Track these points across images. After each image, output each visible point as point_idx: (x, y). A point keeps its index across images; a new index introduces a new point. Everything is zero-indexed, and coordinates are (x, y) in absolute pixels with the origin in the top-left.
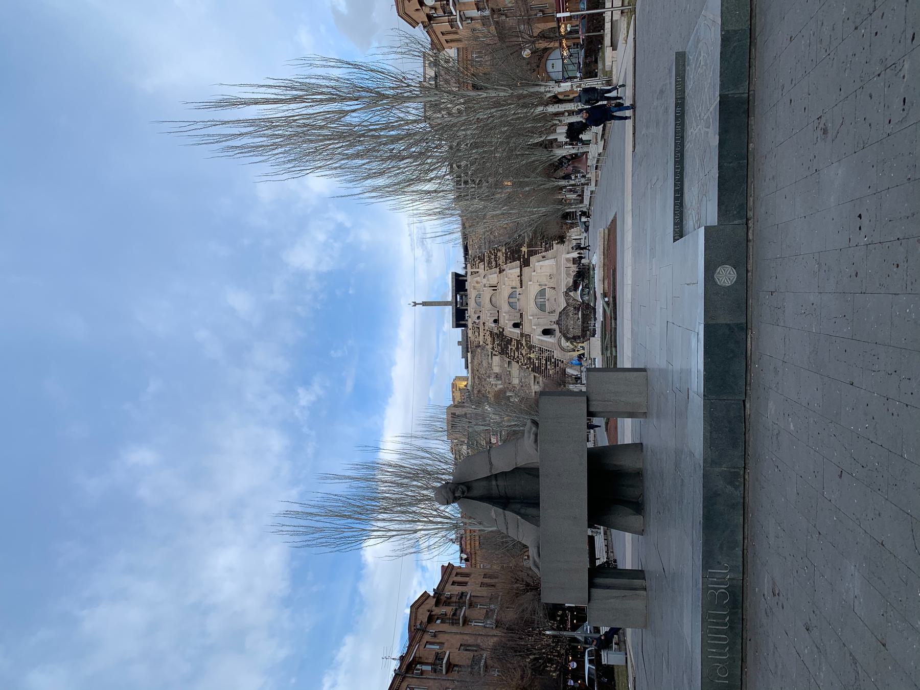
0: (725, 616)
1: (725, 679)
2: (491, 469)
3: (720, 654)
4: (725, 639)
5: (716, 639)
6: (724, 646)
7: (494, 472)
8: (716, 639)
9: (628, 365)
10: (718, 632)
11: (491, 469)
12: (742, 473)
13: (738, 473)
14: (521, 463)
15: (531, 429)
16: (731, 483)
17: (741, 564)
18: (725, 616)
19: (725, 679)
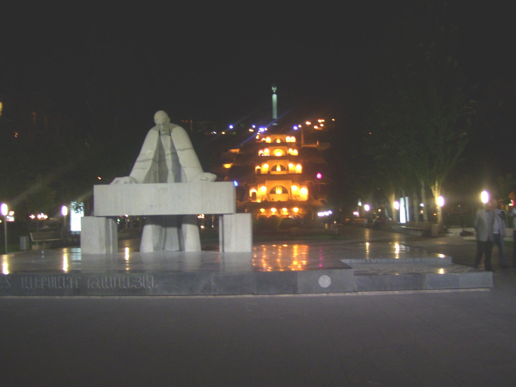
3: (104, 284)
4: (113, 286)
5: (113, 281)
6: (109, 285)
7: (179, 153)
8: (113, 281)
10: (117, 282)
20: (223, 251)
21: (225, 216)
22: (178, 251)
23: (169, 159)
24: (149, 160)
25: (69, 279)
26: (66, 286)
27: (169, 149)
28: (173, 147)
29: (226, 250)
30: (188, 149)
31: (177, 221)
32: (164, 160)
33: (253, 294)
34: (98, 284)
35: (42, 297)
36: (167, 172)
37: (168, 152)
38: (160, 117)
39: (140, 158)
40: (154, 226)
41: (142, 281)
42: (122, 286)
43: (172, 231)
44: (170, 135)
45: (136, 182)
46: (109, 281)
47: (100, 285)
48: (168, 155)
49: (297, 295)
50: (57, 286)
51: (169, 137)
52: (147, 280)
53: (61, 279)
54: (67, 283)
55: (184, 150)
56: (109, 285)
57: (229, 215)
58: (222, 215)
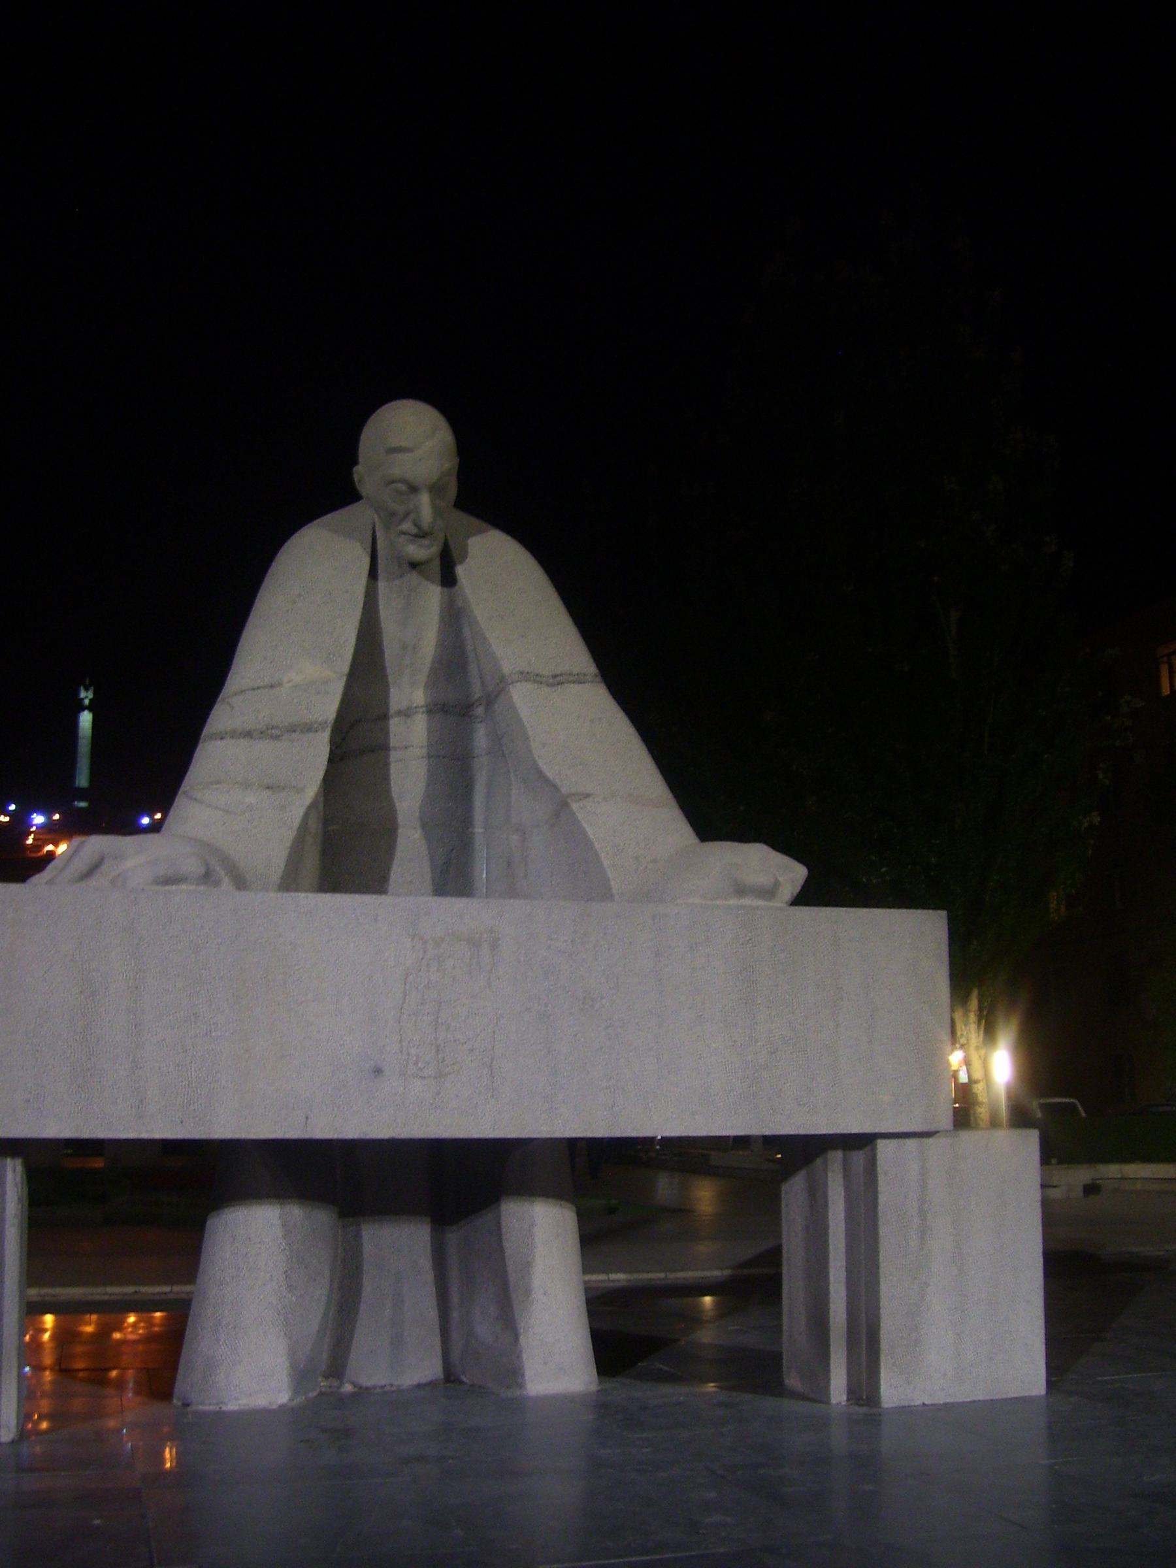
20: (865, 1390)
21: (884, 1148)
22: (432, 1384)
23: (410, 740)
27: (422, 677)
28: (455, 660)
29: (894, 1390)
30: (579, 679)
31: (452, 1185)
32: (382, 748)
36: (388, 831)
37: (409, 692)
38: (410, 441)
39: (221, 718)
40: (296, 1211)
43: (400, 1248)
44: (448, 579)
45: (241, 882)
48: (407, 713)
51: (432, 595)
55: (558, 680)
57: (911, 1143)
58: (863, 1142)
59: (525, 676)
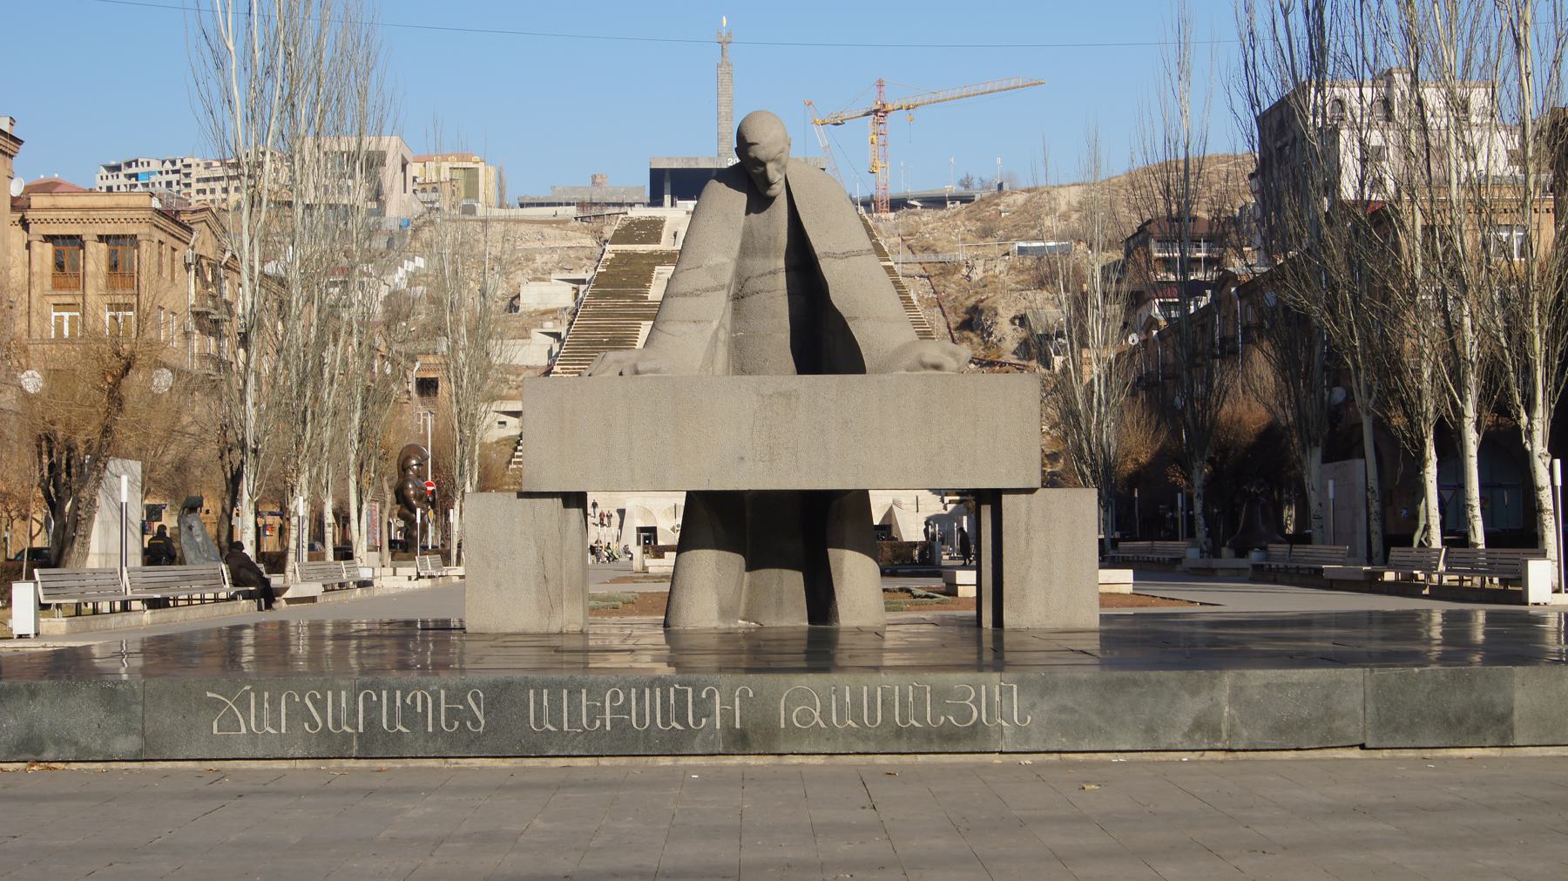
0: (921, 719)
1: (788, 720)
2: (834, 256)
4: (873, 718)
6: (858, 717)
7: (825, 266)
9: (974, 612)
11: (834, 256)
12: (1219, 745)
13: (1218, 739)
14: (862, 332)
15: (953, 355)
16: (1198, 726)
17: (1033, 747)
18: (921, 719)
19: (788, 720)
24: (716, 290)
25: (711, 694)
26: (697, 722)
33: (1362, 747)
34: (817, 714)
35: (604, 762)
41: (977, 701)
42: (904, 720)
46: (856, 703)
47: (826, 714)
49: (1508, 752)
50: (666, 722)
52: (997, 698)
53: (681, 695)
54: (703, 709)
55: (846, 255)
56: (858, 717)
59: (827, 255)
